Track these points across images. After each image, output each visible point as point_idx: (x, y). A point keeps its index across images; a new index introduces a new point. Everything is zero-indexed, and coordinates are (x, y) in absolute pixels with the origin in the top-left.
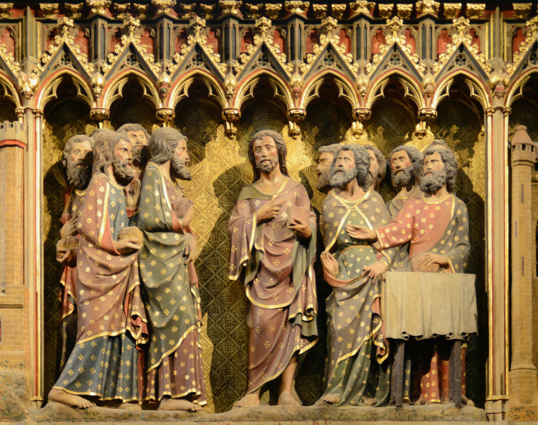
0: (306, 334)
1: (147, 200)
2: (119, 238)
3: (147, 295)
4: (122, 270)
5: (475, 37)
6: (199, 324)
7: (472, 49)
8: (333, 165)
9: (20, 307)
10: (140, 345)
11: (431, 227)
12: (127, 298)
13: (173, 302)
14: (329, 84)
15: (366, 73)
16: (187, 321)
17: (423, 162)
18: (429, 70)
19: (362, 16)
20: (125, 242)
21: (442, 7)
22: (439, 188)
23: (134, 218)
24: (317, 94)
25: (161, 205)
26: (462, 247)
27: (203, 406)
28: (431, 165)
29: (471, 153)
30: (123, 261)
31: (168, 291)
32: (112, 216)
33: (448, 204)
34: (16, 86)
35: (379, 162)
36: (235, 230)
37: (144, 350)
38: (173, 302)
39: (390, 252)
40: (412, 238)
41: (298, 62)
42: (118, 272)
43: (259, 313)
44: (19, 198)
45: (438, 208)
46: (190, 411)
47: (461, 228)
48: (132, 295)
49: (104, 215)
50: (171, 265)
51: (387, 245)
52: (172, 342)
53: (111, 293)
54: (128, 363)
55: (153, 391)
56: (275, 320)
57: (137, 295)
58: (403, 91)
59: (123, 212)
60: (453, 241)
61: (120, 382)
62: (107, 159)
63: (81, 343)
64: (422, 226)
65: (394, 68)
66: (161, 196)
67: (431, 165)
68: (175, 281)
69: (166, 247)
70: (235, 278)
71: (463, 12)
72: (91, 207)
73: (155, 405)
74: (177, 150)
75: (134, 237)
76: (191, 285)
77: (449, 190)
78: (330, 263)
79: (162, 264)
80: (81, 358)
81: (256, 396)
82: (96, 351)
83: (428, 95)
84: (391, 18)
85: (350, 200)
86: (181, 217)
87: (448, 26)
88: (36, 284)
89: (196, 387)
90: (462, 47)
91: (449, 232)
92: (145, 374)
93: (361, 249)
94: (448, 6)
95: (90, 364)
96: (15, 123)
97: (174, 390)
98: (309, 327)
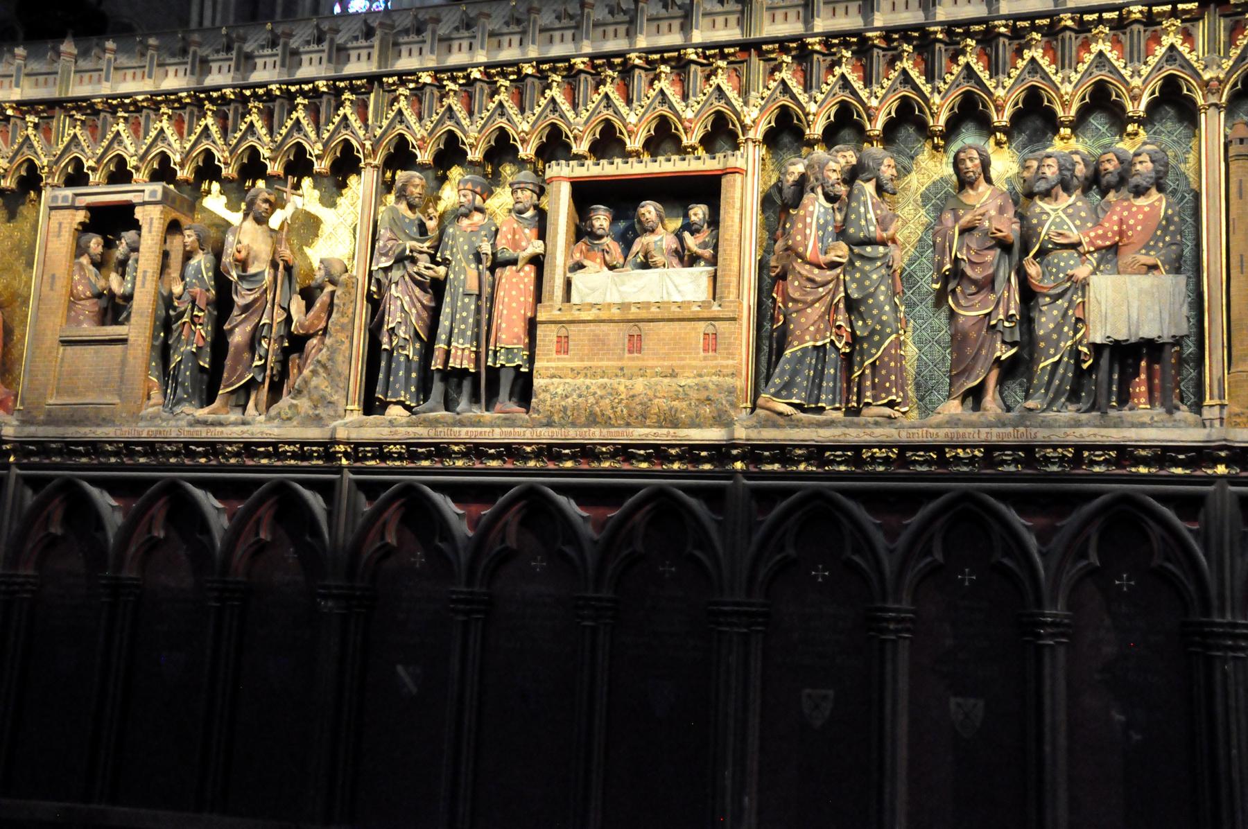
0: (1008, 340)
1: (853, 217)
2: (826, 253)
3: (852, 306)
4: (828, 283)
5: (1188, 36)
6: (902, 332)
7: (1184, 49)
8: (1037, 172)
9: (734, 319)
10: (844, 354)
11: (1139, 228)
12: (832, 308)
13: (875, 312)
15: (1070, 82)
16: (888, 330)
17: (1132, 164)
19: (1066, 28)
20: (832, 257)
21: (1150, 11)
22: (1148, 189)
23: (841, 234)
24: (1020, 105)
25: (866, 220)
26: (1174, 247)
27: (904, 413)
28: (1138, 167)
30: (829, 274)
31: (871, 301)
32: (821, 233)
34: (739, 119)
35: (1086, 165)
36: (939, 240)
37: (848, 360)
38: (875, 312)
39: (1096, 255)
40: (1120, 240)
41: (1001, 77)
42: (824, 285)
43: (961, 320)
44: (737, 220)
45: (1147, 209)
46: (890, 417)
47: (1172, 228)
48: (837, 305)
50: (875, 277)
51: (1092, 249)
52: (874, 351)
53: (817, 305)
54: (832, 371)
55: (855, 398)
56: (976, 328)
57: (841, 306)
58: (1110, 95)
59: (830, 229)
60: (1164, 241)
61: (824, 389)
62: (817, 180)
63: (788, 353)
64: (1130, 227)
65: (1099, 75)
66: (867, 211)
67: (1138, 167)
68: (878, 292)
69: (871, 260)
70: (937, 286)
71: (1174, 14)
72: (800, 226)
73: (857, 412)
74: (883, 168)
75: (841, 251)
76: (895, 294)
77: (1161, 189)
78: (1033, 270)
79: (866, 275)
80: (787, 367)
81: (957, 402)
82: (800, 360)
83: (1135, 98)
84: (1096, 27)
85: (1054, 206)
86: (885, 230)
87: (1158, 28)
88: (749, 298)
89: (897, 394)
90: (1172, 47)
91: (1159, 233)
92: (849, 381)
93: (1065, 253)
94: (1156, 9)
95: (795, 373)
96: (738, 153)
97: (875, 398)
98: (1012, 333)
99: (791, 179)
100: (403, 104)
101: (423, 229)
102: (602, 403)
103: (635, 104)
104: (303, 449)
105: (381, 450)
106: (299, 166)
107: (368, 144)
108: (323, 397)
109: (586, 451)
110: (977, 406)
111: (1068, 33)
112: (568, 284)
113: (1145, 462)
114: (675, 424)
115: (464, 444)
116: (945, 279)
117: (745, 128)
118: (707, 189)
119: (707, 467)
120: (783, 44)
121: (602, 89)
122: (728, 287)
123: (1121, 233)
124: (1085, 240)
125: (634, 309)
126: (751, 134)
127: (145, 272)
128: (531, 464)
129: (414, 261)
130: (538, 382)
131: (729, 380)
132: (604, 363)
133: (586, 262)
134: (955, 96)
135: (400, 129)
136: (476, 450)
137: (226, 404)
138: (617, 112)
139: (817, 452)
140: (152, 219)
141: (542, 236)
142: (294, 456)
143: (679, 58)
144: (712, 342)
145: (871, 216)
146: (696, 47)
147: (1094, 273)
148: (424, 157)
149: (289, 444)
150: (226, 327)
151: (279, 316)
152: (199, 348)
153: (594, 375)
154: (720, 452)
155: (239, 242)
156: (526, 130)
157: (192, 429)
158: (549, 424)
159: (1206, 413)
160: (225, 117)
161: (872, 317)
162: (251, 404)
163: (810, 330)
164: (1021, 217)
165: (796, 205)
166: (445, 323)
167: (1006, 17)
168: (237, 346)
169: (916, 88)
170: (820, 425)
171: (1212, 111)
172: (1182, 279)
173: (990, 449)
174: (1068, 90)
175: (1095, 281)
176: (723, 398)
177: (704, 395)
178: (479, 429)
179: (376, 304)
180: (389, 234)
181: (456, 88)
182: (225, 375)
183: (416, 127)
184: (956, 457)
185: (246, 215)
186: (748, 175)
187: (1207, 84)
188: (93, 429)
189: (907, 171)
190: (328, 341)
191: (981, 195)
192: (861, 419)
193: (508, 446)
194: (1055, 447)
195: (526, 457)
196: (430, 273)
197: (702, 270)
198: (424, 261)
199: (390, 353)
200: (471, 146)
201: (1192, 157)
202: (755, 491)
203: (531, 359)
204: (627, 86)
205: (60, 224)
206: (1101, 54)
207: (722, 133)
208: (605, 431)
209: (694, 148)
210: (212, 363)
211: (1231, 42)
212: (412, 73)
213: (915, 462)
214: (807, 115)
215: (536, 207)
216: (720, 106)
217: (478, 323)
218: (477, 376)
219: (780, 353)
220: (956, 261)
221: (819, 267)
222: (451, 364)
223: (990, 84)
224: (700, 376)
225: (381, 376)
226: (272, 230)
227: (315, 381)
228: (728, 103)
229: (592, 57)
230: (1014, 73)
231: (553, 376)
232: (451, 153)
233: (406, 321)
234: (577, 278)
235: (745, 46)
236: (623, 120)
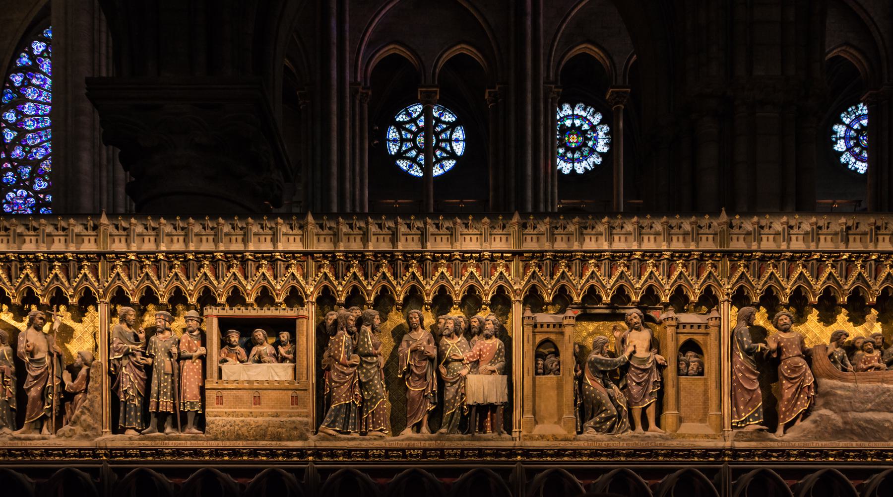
5: (507, 268)
7: (506, 274)
12: (352, 386)
14: (442, 289)
17: (485, 324)
18: (487, 283)
19: (457, 259)
20: (352, 361)
23: (355, 351)
29: (507, 318)
30: (351, 370)
33: (496, 342)
42: (349, 374)
49: (342, 349)
64: (484, 353)
65: (471, 282)
69: (371, 364)
73: (365, 434)
75: (356, 359)
78: (443, 371)
83: (487, 295)
88: (313, 380)
90: (501, 273)
92: (361, 419)
93: (457, 364)
94: (495, 255)
97: (374, 427)
99: (331, 322)
100: (119, 270)
101: (137, 338)
102: (243, 429)
103: (250, 279)
104: (81, 452)
105: (125, 452)
106: (59, 298)
107: (101, 291)
108: (89, 426)
109: (235, 452)
110: (418, 431)
111: (457, 262)
112: (220, 370)
113: (490, 455)
114: (280, 439)
116: (404, 374)
117: (307, 295)
118: (290, 325)
119: (295, 459)
120: (325, 255)
121: (232, 270)
122: (302, 374)
123: (480, 355)
124: (465, 358)
125: (255, 384)
126: (310, 299)
128: (207, 458)
129: (134, 355)
130: (208, 419)
131: (305, 419)
132: (242, 410)
133: (228, 359)
134: (407, 287)
135: (118, 283)
136: (177, 452)
137: (29, 429)
138: (240, 283)
139: (348, 453)
141: (204, 344)
142: (75, 455)
143: (272, 257)
144: (295, 401)
145: (370, 342)
146: (280, 252)
147: (469, 373)
148: (135, 299)
149: (72, 449)
150: (25, 387)
151: (57, 382)
152: (9, 398)
153: (237, 416)
154: (302, 453)
155: (27, 341)
156: (192, 289)
158: (216, 439)
159: (514, 435)
160: (9, 269)
161: (372, 390)
162: (45, 428)
163: (342, 397)
164: (437, 344)
165: (334, 334)
166: (154, 388)
167: (430, 251)
168: (34, 398)
169: (389, 282)
170: (349, 440)
171: (517, 303)
172: (505, 377)
173: (425, 450)
174: (458, 289)
175: (469, 376)
176: (303, 428)
177: (293, 426)
179: (114, 378)
180: (119, 341)
181: (150, 263)
182: (28, 413)
183: (128, 283)
184: (411, 454)
185: (29, 326)
186: (308, 319)
187: (515, 291)
189: (386, 320)
190: (89, 396)
191: (419, 335)
192: (367, 437)
193: (195, 450)
194: (453, 450)
195: (204, 455)
196: (144, 362)
197: (288, 365)
198: (139, 357)
199: (125, 403)
200: (161, 295)
201: (509, 321)
202: (319, 470)
203: (203, 407)
204: (244, 269)
206: (472, 273)
207: (295, 298)
208: (245, 443)
209: (281, 304)
210: (18, 406)
211: (525, 273)
212: (124, 253)
213: (393, 456)
214: (338, 291)
215: (199, 329)
216: (294, 283)
217: (173, 388)
218: (174, 416)
219: (329, 407)
220: (409, 365)
221: (346, 366)
222: (161, 409)
223: (424, 283)
224: (291, 416)
225: (121, 415)
226: (45, 334)
227: (83, 417)
228: (298, 282)
229: (226, 253)
230: (434, 278)
232: (149, 297)
233: (132, 387)
234: (225, 367)
235: (306, 254)
236: (244, 287)
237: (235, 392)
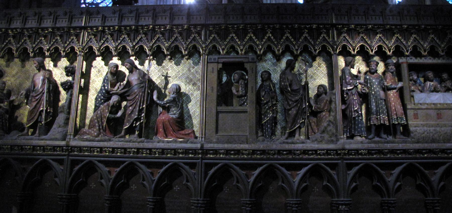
109: (430, 151)
115: (389, 149)
125: (439, 105)
127: (252, 87)
136: (393, 151)
140: (252, 68)
142: (324, 154)
149: (322, 150)
153: (429, 127)
157: (282, 145)
158: (418, 142)
178: (394, 144)
188: (239, 145)
205: (213, 68)
208: (437, 145)
231: (415, 127)
237: (425, 110)
